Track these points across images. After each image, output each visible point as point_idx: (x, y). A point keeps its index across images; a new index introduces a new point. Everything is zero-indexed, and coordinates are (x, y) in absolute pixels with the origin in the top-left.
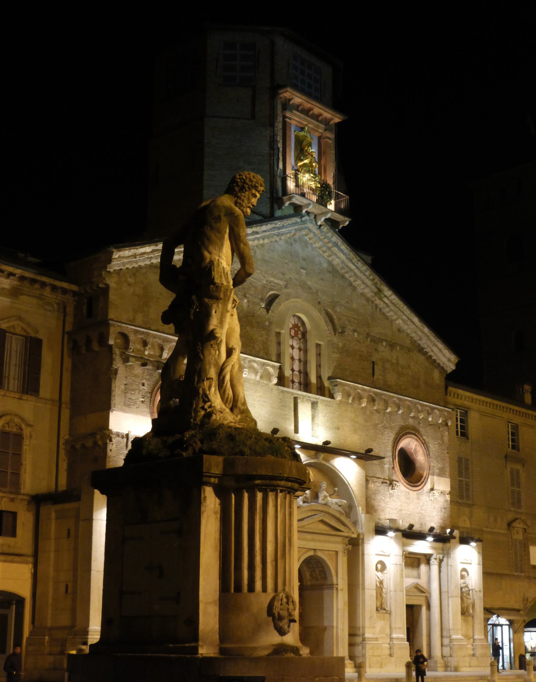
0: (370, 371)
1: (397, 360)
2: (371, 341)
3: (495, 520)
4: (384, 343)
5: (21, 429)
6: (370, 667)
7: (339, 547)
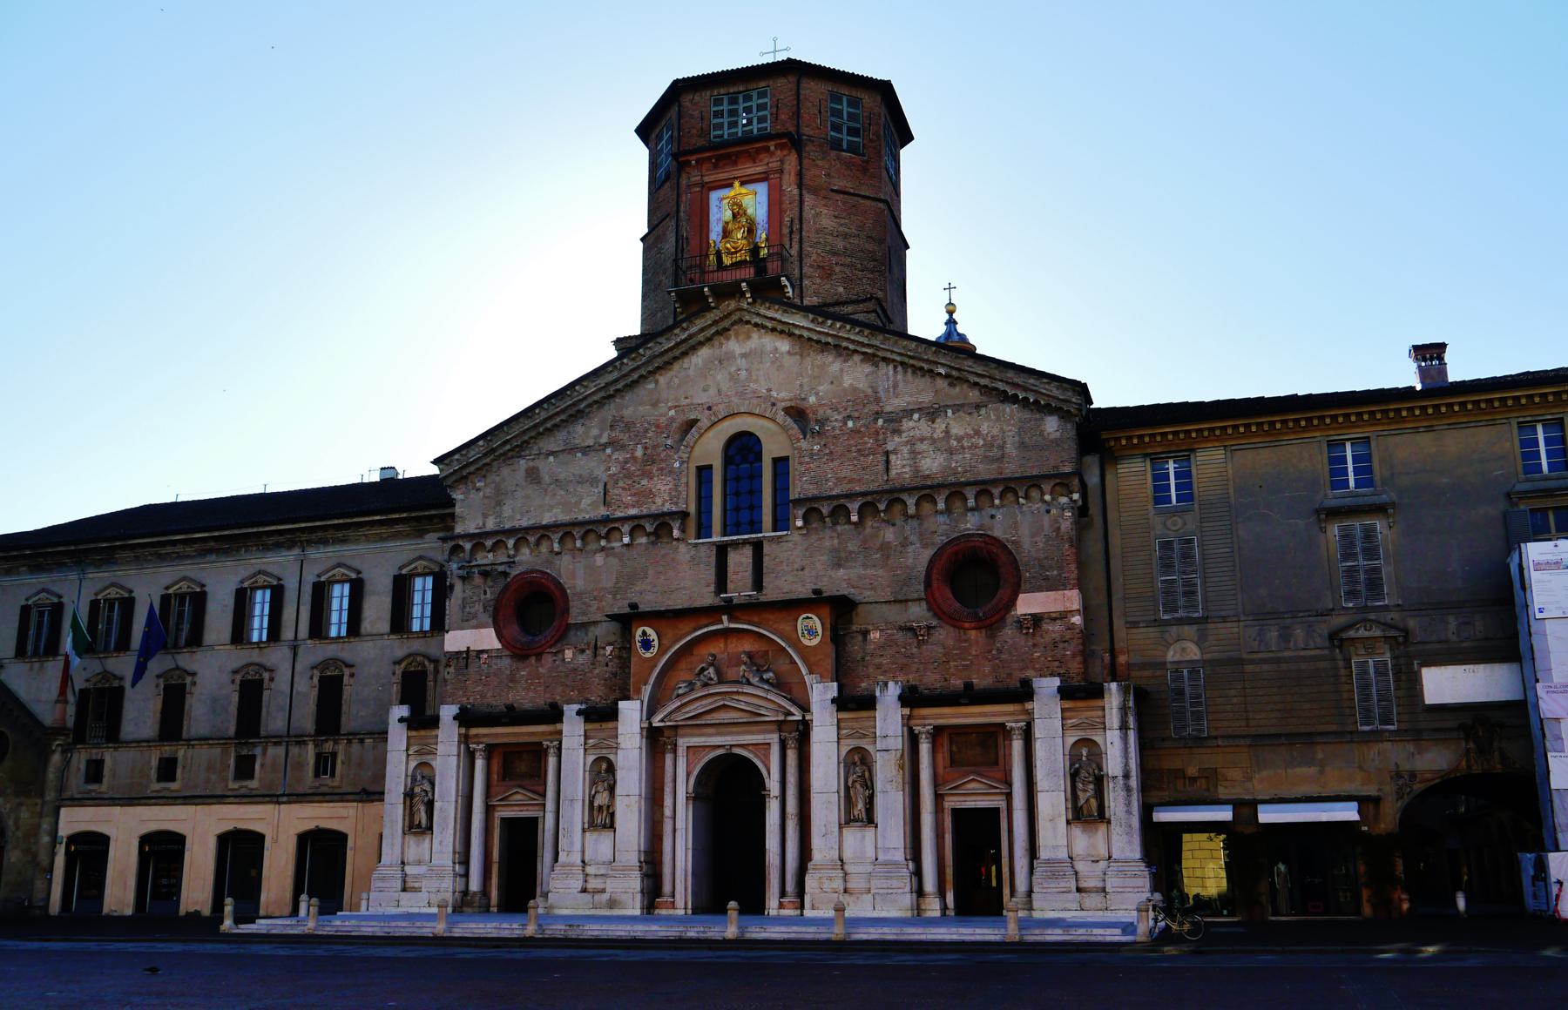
0: (881, 467)
1: (947, 432)
3: (1285, 636)
4: (916, 416)
6: (813, 908)
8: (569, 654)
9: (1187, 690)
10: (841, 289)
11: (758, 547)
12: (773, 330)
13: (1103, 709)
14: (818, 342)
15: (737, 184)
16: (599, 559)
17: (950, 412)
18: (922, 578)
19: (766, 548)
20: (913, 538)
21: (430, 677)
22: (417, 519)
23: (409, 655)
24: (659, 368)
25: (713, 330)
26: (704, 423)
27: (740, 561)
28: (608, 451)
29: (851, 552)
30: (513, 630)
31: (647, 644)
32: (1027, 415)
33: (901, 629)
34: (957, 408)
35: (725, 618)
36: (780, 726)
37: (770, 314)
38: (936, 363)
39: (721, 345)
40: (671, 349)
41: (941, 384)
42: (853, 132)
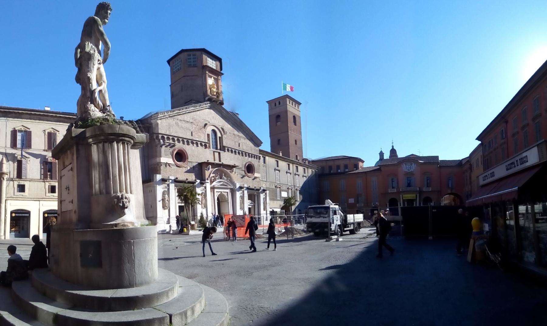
7: (228, 191)
11: (219, 153)
19: (221, 154)
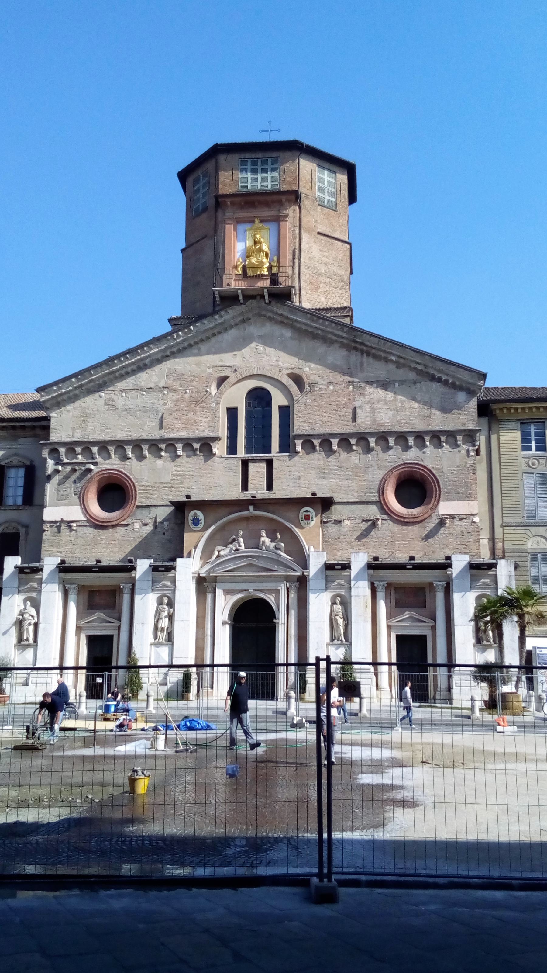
2: (353, 387)
5: (18, 530)
8: (137, 526)
9: (541, 567)
10: (323, 299)
11: (270, 463)
12: (282, 323)
13: (496, 576)
14: (311, 333)
15: (257, 221)
16: (159, 463)
17: (397, 385)
18: (377, 489)
19: (275, 465)
20: (373, 463)
21: (22, 538)
22: (14, 428)
23: (6, 522)
24: (202, 340)
25: (240, 319)
26: (233, 378)
27: (257, 471)
28: (166, 392)
29: (331, 470)
30: (95, 508)
31: (196, 522)
32: (445, 390)
33: (364, 521)
34: (402, 382)
35: (251, 508)
36: (287, 579)
37: (280, 311)
38: (391, 354)
39: (245, 329)
40: (211, 329)
41: (392, 367)
42: (331, 194)
